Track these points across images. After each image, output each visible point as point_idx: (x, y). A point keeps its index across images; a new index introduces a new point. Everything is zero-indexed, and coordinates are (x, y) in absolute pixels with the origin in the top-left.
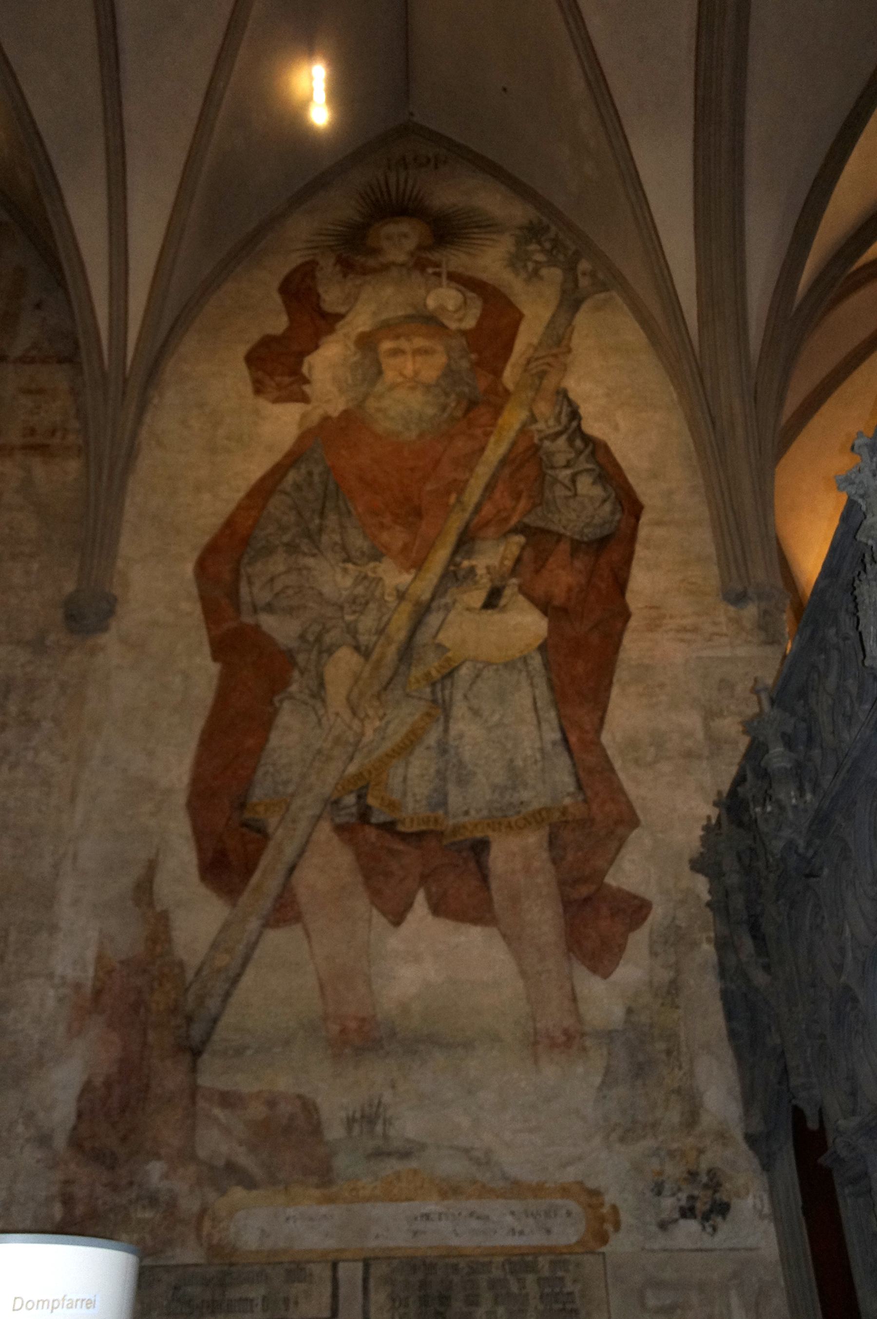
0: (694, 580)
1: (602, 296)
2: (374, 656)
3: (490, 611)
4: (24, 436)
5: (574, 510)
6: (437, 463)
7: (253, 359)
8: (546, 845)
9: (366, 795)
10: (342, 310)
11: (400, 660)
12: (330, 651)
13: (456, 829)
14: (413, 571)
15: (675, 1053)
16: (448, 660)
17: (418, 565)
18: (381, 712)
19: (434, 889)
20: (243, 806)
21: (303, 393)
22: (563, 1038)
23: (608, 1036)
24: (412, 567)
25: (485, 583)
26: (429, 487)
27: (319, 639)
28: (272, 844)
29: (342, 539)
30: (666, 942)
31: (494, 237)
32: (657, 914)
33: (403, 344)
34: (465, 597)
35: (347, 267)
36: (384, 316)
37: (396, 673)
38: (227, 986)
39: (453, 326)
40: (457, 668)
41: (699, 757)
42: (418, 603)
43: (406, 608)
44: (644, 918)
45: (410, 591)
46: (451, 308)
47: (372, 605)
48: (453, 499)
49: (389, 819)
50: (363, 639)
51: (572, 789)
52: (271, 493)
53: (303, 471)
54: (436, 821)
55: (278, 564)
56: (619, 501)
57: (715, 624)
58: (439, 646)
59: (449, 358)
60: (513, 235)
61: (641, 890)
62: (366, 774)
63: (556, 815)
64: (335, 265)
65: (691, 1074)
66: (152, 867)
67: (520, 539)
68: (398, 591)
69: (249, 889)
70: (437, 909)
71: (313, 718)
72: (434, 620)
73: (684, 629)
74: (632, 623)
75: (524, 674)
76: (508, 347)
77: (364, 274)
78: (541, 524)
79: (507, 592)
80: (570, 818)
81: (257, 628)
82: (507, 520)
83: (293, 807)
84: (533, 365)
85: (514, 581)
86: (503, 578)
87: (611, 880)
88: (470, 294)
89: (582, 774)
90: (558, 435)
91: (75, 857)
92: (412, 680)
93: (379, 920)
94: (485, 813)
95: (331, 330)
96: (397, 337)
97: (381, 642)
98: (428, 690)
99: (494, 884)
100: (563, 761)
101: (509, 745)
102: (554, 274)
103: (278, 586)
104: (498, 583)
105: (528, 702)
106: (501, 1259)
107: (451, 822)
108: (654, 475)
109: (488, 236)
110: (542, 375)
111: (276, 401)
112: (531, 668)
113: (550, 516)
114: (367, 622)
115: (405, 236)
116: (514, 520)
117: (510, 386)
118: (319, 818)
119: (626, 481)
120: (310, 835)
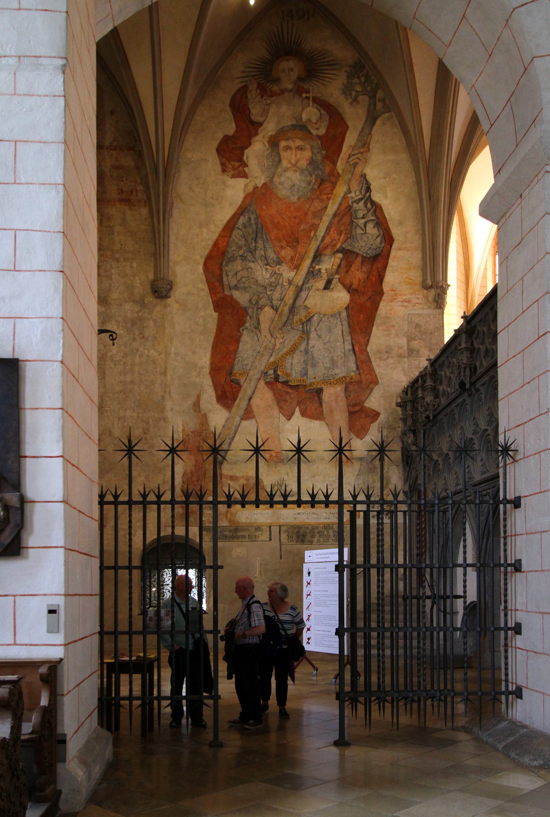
0: (411, 278)
2: (280, 311)
4: (119, 194)
5: (364, 241)
6: (306, 214)
7: (219, 151)
10: (260, 119)
11: (290, 313)
12: (262, 308)
13: (310, 385)
14: (295, 270)
16: (309, 313)
17: (297, 267)
18: (282, 336)
20: (231, 374)
21: (245, 172)
24: (295, 268)
25: (325, 277)
26: (302, 227)
27: (257, 303)
28: (242, 389)
29: (265, 253)
31: (336, 72)
32: (382, 417)
33: (291, 143)
35: (263, 91)
36: (282, 125)
37: (288, 319)
38: (229, 441)
39: (314, 132)
40: (312, 317)
41: (404, 357)
42: (297, 286)
43: (292, 288)
44: (377, 419)
45: (294, 280)
46: (314, 121)
47: (278, 287)
48: (313, 233)
49: (285, 380)
50: (275, 303)
51: (355, 369)
52: (233, 229)
53: (246, 217)
54: (303, 381)
55: (238, 265)
56: (384, 236)
57: (418, 299)
58: (305, 306)
59: (313, 153)
60: (346, 71)
62: (277, 362)
63: (348, 379)
64: (257, 89)
66: (199, 397)
67: (340, 255)
68: (289, 280)
70: (304, 414)
71: (256, 338)
72: (303, 294)
73: (404, 301)
74: (384, 298)
75: (339, 320)
77: (272, 96)
78: (349, 248)
79: (334, 282)
82: (335, 245)
83: (249, 375)
85: (337, 276)
86: (332, 275)
88: (323, 111)
89: (359, 364)
90: (360, 200)
91: (170, 393)
92: (295, 321)
93: (283, 418)
95: (256, 134)
96: (288, 139)
97: (282, 304)
98: (301, 326)
99: (324, 406)
100: (352, 358)
101: (332, 350)
102: (364, 99)
103: (239, 277)
104: (330, 277)
105: (340, 332)
106: (322, 526)
107: (309, 381)
108: (400, 223)
109: (333, 72)
110: (355, 165)
111: (233, 177)
113: (354, 244)
114: (276, 295)
115: (292, 70)
116: (338, 247)
117: (340, 171)
118: (260, 379)
119: (388, 225)
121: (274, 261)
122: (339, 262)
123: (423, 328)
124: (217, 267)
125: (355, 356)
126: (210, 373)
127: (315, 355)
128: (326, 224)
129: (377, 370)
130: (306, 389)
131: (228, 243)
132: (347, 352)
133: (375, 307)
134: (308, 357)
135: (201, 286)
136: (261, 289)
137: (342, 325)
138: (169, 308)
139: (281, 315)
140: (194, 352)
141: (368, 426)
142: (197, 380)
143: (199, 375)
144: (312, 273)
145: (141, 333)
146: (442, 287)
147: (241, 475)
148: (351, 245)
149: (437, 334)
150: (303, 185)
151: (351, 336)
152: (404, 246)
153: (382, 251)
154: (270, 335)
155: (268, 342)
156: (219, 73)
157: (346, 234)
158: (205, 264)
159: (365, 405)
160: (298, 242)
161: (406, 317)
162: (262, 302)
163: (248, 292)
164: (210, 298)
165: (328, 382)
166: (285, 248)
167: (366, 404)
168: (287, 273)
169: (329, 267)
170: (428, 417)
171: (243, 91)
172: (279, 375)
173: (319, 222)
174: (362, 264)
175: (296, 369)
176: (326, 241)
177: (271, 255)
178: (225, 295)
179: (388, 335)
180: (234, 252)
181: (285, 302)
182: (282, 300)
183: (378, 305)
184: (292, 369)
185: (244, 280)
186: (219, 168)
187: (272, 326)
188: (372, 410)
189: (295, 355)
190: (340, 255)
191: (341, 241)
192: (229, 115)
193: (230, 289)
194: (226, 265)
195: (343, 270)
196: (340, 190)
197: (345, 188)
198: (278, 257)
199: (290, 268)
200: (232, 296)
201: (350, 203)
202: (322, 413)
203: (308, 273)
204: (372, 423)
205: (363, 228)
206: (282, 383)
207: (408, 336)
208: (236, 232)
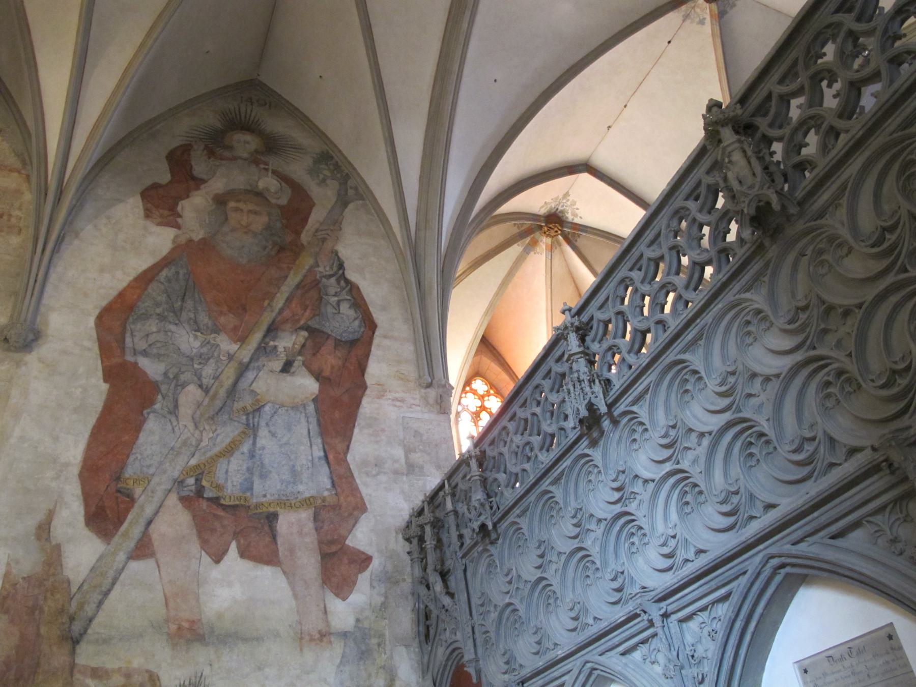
1: (361, 202)
2: (211, 393)
3: (285, 374)
8: (312, 519)
9: (202, 479)
10: (205, 177)
11: (228, 397)
12: (183, 386)
13: (257, 506)
14: (239, 343)
15: (383, 645)
16: (258, 401)
17: (242, 340)
18: (214, 428)
19: (242, 541)
20: (118, 479)
21: (177, 222)
22: (317, 636)
23: (345, 635)
24: (237, 341)
25: (283, 358)
27: (176, 377)
28: (136, 505)
29: (195, 316)
30: (380, 581)
32: (376, 564)
33: (241, 205)
34: (270, 364)
35: (211, 153)
38: (100, 597)
39: (273, 201)
40: (263, 406)
41: (403, 474)
44: (368, 566)
45: (236, 355)
47: (212, 361)
48: (266, 303)
49: (215, 496)
50: (205, 381)
51: (329, 486)
52: (151, 280)
53: (173, 270)
55: (152, 326)
57: (414, 399)
58: (253, 392)
59: (270, 219)
62: (202, 466)
63: (320, 501)
64: (203, 150)
65: (391, 657)
68: (229, 354)
69: (119, 533)
70: (243, 554)
71: (169, 427)
72: (250, 375)
73: (397, 399)
74: (368, 392)
75: (304, 415)
76: (305, 220)
78: (317, 326)
79: (296, 364)
80: (327, 504)
81: (135, 364)
82: (298, 321)
83: (152, 483)
84: (319, 233)
85: (300, 358)
87: (348, 542)
88: (283, 184)
89: (335, 479)
90: (331, 276)
93: (206, 559)
94: (276, 496)
96: (238, 201)
97: (216, 384)
98: (244, 417)
100: (325, 470)
101: (292, 457)
103: (152, 339)
104: (290, 358)
105: (305, 432)
107: (255, 500)
108: (384, 308)
109: (297, 154)
110: (324, 240)
112: (307, 411)
115: (248, 143)
116: (302, 322)
117: (305, 243)
118: (170, 491)
119: (368, 309)
120: (163, 501)
122: (303, 341)
123: (424, 438)
124: (118, 323)
125: (329, 467)
126: (81, 475)
128: (286, 295)
129: (364, 491)
130: (250, 513)
131: (140, 297)
132: (316, 460)
133: (356, 403)
135: (87, 344)
137: (308, 422)
138: (24, 368)
139: (214, 397)
140: (56, 439)
142: (53, 484)
143: (57, 478)
144: (264, 350)
147: (117, 667)
149: (444, 446)
151: (323, 438)
153: (362, 336)
154: (192, 424)
155: (189, 434)
156: (158, 127)
158: (100, 319)
160: (245, 309)
161: (401, 421)
162: (186, 376)
163: (163, 361)
164: (100, 362)
165: (288, 504)
167: (348, 542)
168: (226, 345)
169: (290, 345)
171: (186, 149)
172: (203, 487)
174: (335, 348)
175: (234, 479)
179: (377, 442)
183: (361, 402)
184: (227, 479)
185: (159, 345)
186: (140, 211)
187: (198, 413)
188: (359, 551)
189: (232, 459)
192: (164, 166)
193: (135, 354)
194: (133, 323)
196: (307, 261)
198: (215, 324)
203: (258, 349)
205: (335, 306)
208: (154, 285)
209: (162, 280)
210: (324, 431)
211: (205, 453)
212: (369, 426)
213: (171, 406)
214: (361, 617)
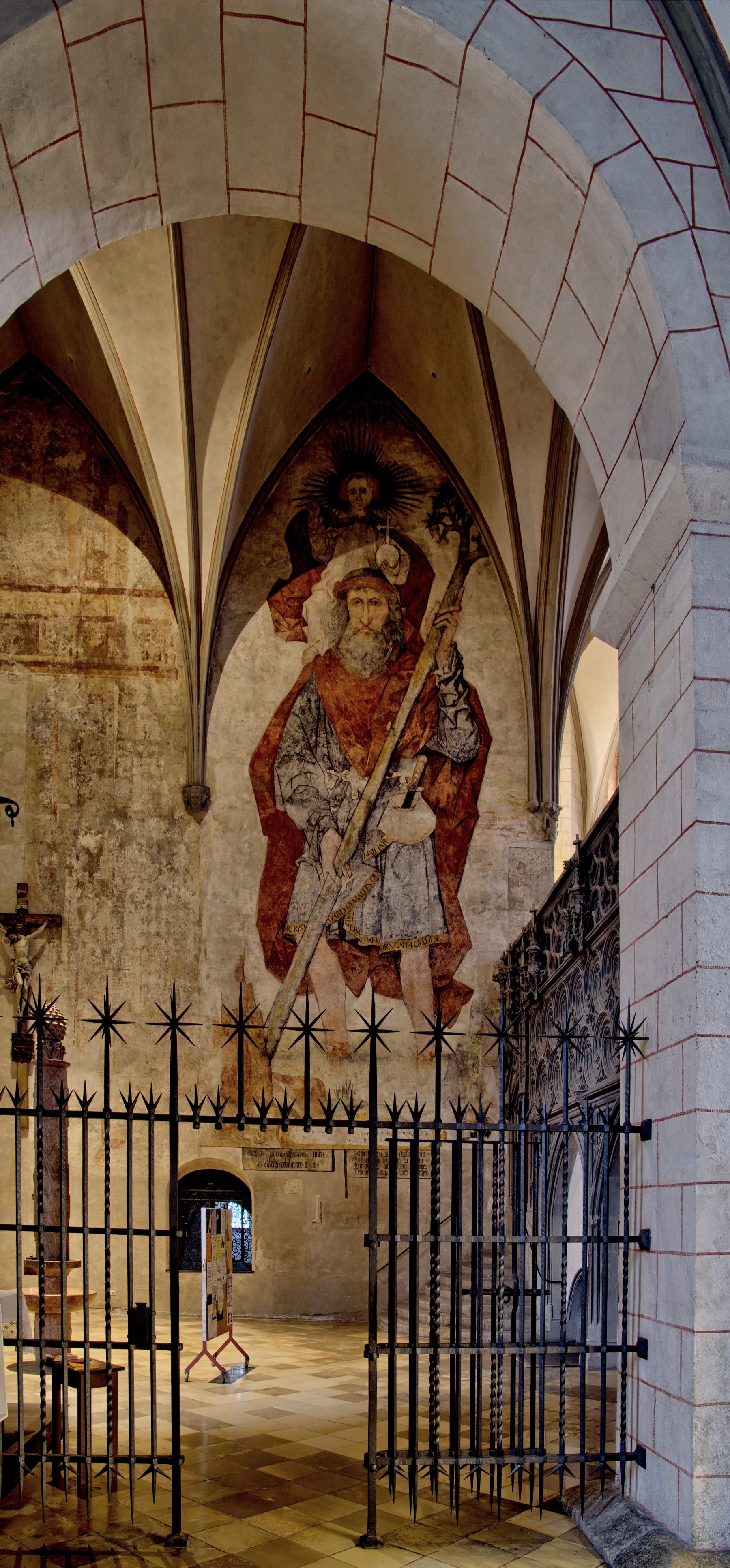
11: (360, 840)
13: (385, 947)
14: (367, 778)
17: (369, 774)
24: (366, 775)
25: (404, 788)
27: (318, 824)
32: (475, 997)
37: (357, 849)
40: (388, 847)
42: (369, 802)
43: (363, 804)
44: (469, 999)
47: (345, 802)
50: (340, 824)
51: (442, 925)
53: (305, 698)
55: (293, 768)
56: (479, 734)
58: (379, 831)
61: (471, 985)
63: (434, 940)
67: (424, 759)
72: (377, 813)
73: (505, 828)
74: (479, 822)
78: (436, 748)
79: (416, 796)
80: (439, 942)
82: (418, 744)
85: (420, 789)
86: (414, 787)
89: (447, 917)
90: (449, 680)
97: (350, 827)
98: (374, 860)
99: (403, 977)
100: (439, 909)
108: (500, 716)
110: (443, 629)
116: (421, 746)
117: (424, 638)
121: (339, 763)
127: (392, 904)
129: (471, 928)
131: (281, 735)
134: (382, 906)
136: (323, 804)
141: (457, 1009)
144: (388, 784)
145: (169, 863)
146: (551, 809)
148: (437, 744)
150: (378, 655)
151: (438, 877)
152: (504, 749)
157: (431, 727)
159: (455, 977)
163: (306, 807)
166: (354, 745)
167: (455, 977)
168: (355, 780)
170: (531, 996)
173: (396, 710)
175: (368, 922)
176: (405, 738)
177: (337, 755)
178: (277, 811)
180: (289, 749)
181: (353, 824)
182: (349, 821)
187: (337, 859)
189: (365, 903)
190: (424, 759)
191: (425, 738)
193: (283, 802)
194: (278, 767)
195: (427, 781)
196: (424, 664)
197: (430, 662)
198: (345, 759)
199: (360, 774)
200: (286, 812)
201: (437, 684)
202: (399, 987)
204: (463, 1004)
205: (453, 719)
206: (349, 942)
207: (509, 879)
209: (298, 712)
210: (439, 870)
211: (345, 897)
212: (479, 860)
213: (316, 853)
214: (461, 1042)
